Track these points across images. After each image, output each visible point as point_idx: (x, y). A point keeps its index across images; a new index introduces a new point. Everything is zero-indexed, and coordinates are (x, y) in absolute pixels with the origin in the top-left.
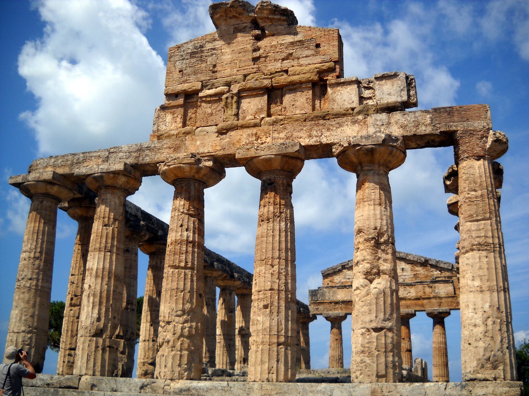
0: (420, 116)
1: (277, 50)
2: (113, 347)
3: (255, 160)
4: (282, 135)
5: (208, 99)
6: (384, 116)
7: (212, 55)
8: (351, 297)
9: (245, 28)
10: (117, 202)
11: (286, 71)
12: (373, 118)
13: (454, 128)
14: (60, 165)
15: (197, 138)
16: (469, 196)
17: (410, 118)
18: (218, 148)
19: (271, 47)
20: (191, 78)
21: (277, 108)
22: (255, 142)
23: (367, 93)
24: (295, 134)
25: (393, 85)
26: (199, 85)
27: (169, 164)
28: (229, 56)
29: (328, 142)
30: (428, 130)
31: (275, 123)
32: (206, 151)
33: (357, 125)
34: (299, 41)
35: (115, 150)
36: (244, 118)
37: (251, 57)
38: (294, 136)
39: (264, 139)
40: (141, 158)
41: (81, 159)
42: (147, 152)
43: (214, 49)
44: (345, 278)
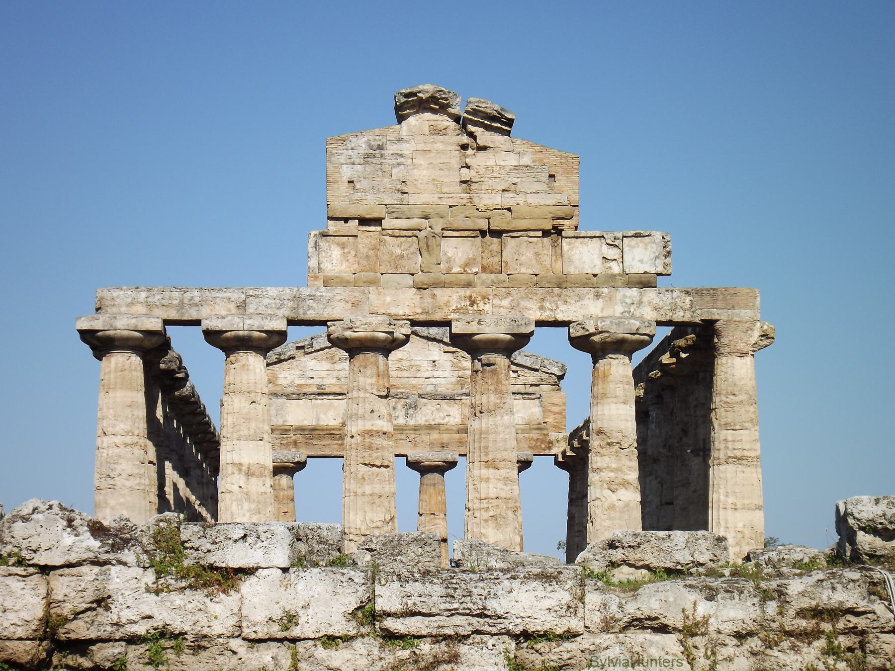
0: (678, 297)
1: (495, 175)
3: (476, 337)
4: (506, 303)
6: (634, 292)
7: (399, 164)
8: (318, 420)
11: (509, 210)
12: (622, 293)
13: (717, 317)
14: (158, 303)
15: (386, 291)
16: (728, 400)
18: (419, 310)
20: (368, 197)
21: (492, 259)
22: (470, 308)
24: (524, 303)
25: (646, 249)
28: (425, 172)
32: (401, 313)
33: (601, 300)
36: (450, 269)
37: (458, 180)
38: (521, 306)
39: (481, 304)
40: (301, 311)
41: (197, 299)
43: (401, 156)
44: (302, 375)
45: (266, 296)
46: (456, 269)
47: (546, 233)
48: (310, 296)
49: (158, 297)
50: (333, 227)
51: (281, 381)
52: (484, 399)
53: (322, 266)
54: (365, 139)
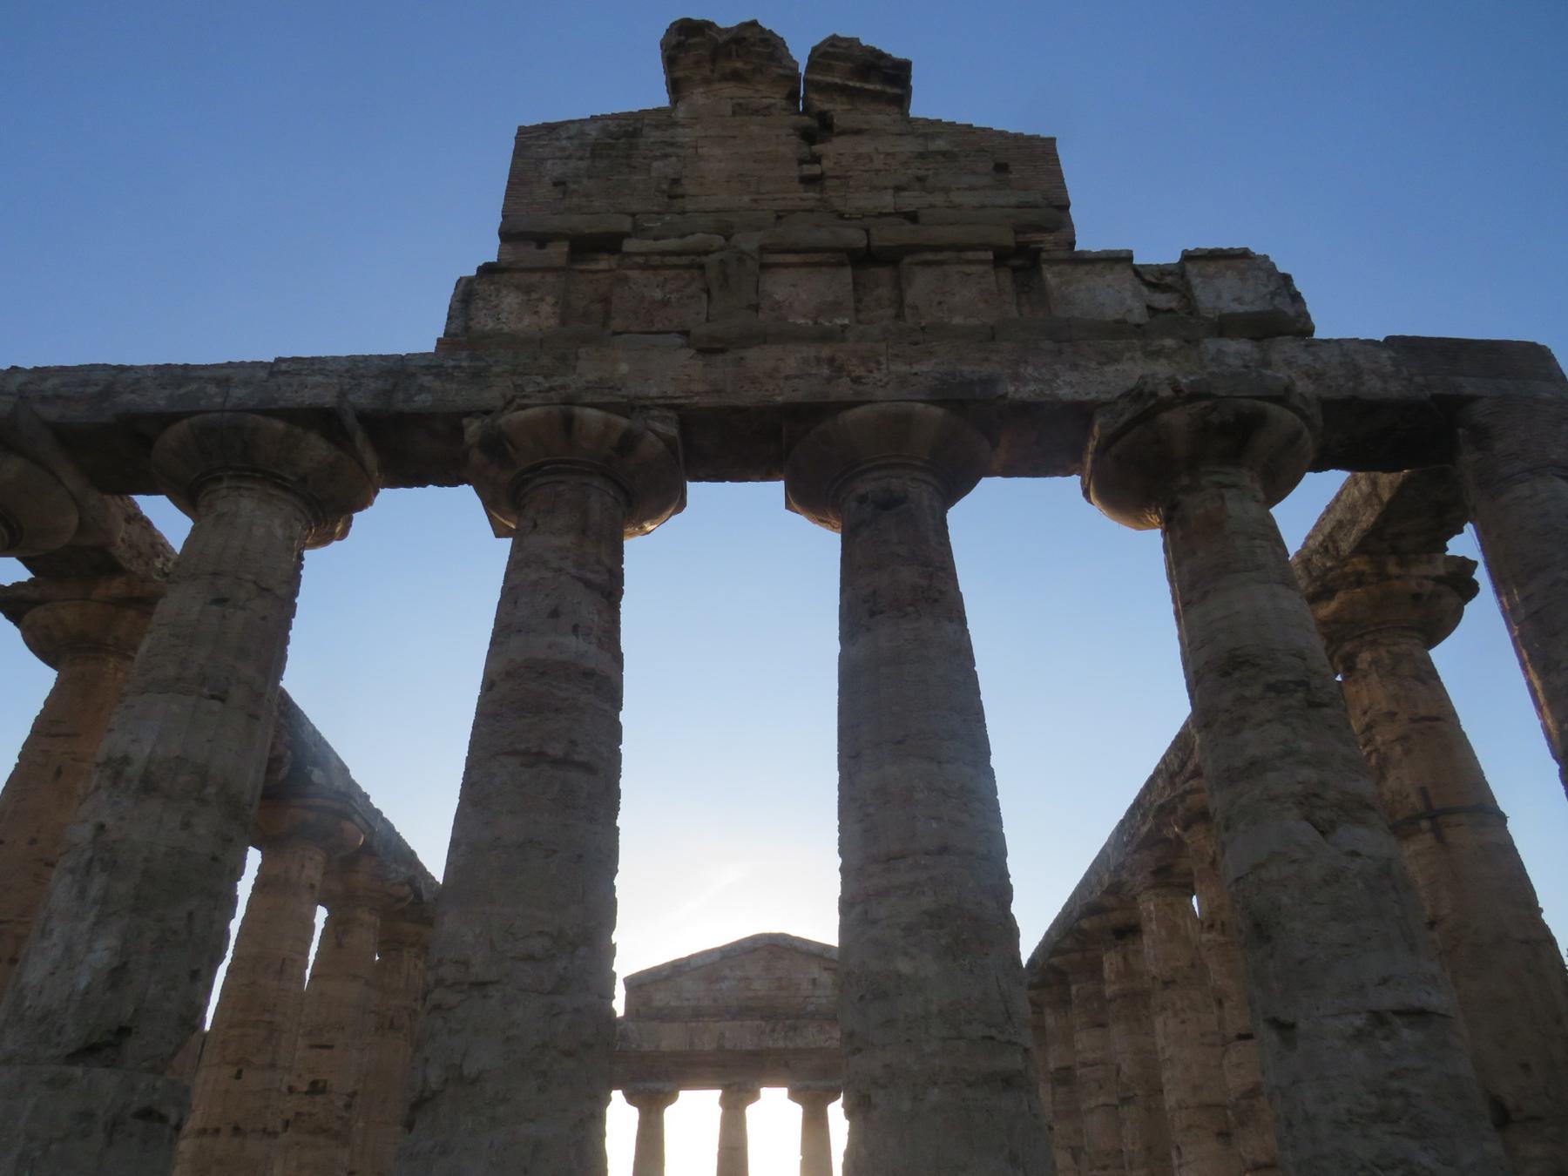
2: (162, 1119)
6: (1237, 349)
7: (666, 156)
9: (768, 107)
10: (279, 532)
11: (912, 217)
18: (699, 387)
19: (859, 157)
23: (1162, 300)
27: (525, 401)
29: (1077, 398)
30: (1395, 389)
32: (654, 392)
34: (944, 154)
35: (294, 366)
42: (427, 380)
43: (672, 145)
47: (1001, 257)
48: (427, 367)
53: (472, 323)
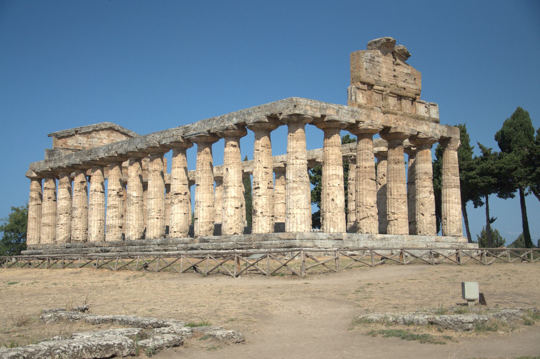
4: (405, 122)
5: (377, 91)
6: (434, 124)
7: (378, 65)
11: (405, 89)
17: (442, 127)
24: (409, 124)
26: (374, 83)
31: (402, 115)
41: (325, 107)
44: (77, 142)
45: (344, 109)
46: (391, 108)
49: (313, 104)
50: (361, 86)
51: (69, 144)
52: (400, 157)
54: (370, 54)
